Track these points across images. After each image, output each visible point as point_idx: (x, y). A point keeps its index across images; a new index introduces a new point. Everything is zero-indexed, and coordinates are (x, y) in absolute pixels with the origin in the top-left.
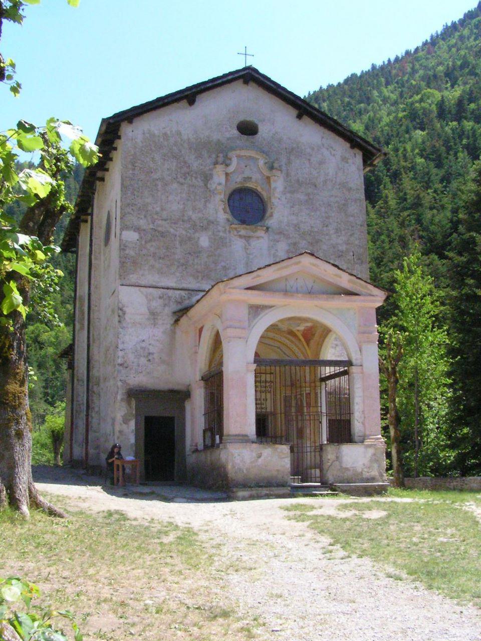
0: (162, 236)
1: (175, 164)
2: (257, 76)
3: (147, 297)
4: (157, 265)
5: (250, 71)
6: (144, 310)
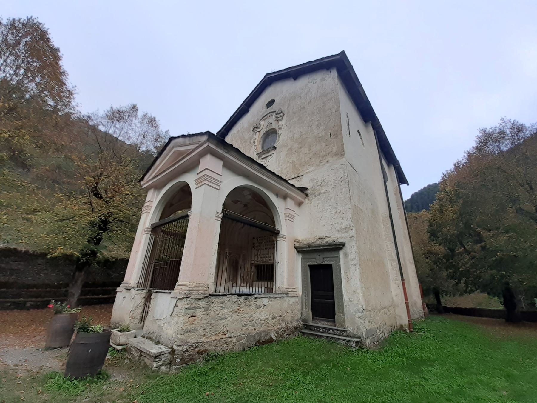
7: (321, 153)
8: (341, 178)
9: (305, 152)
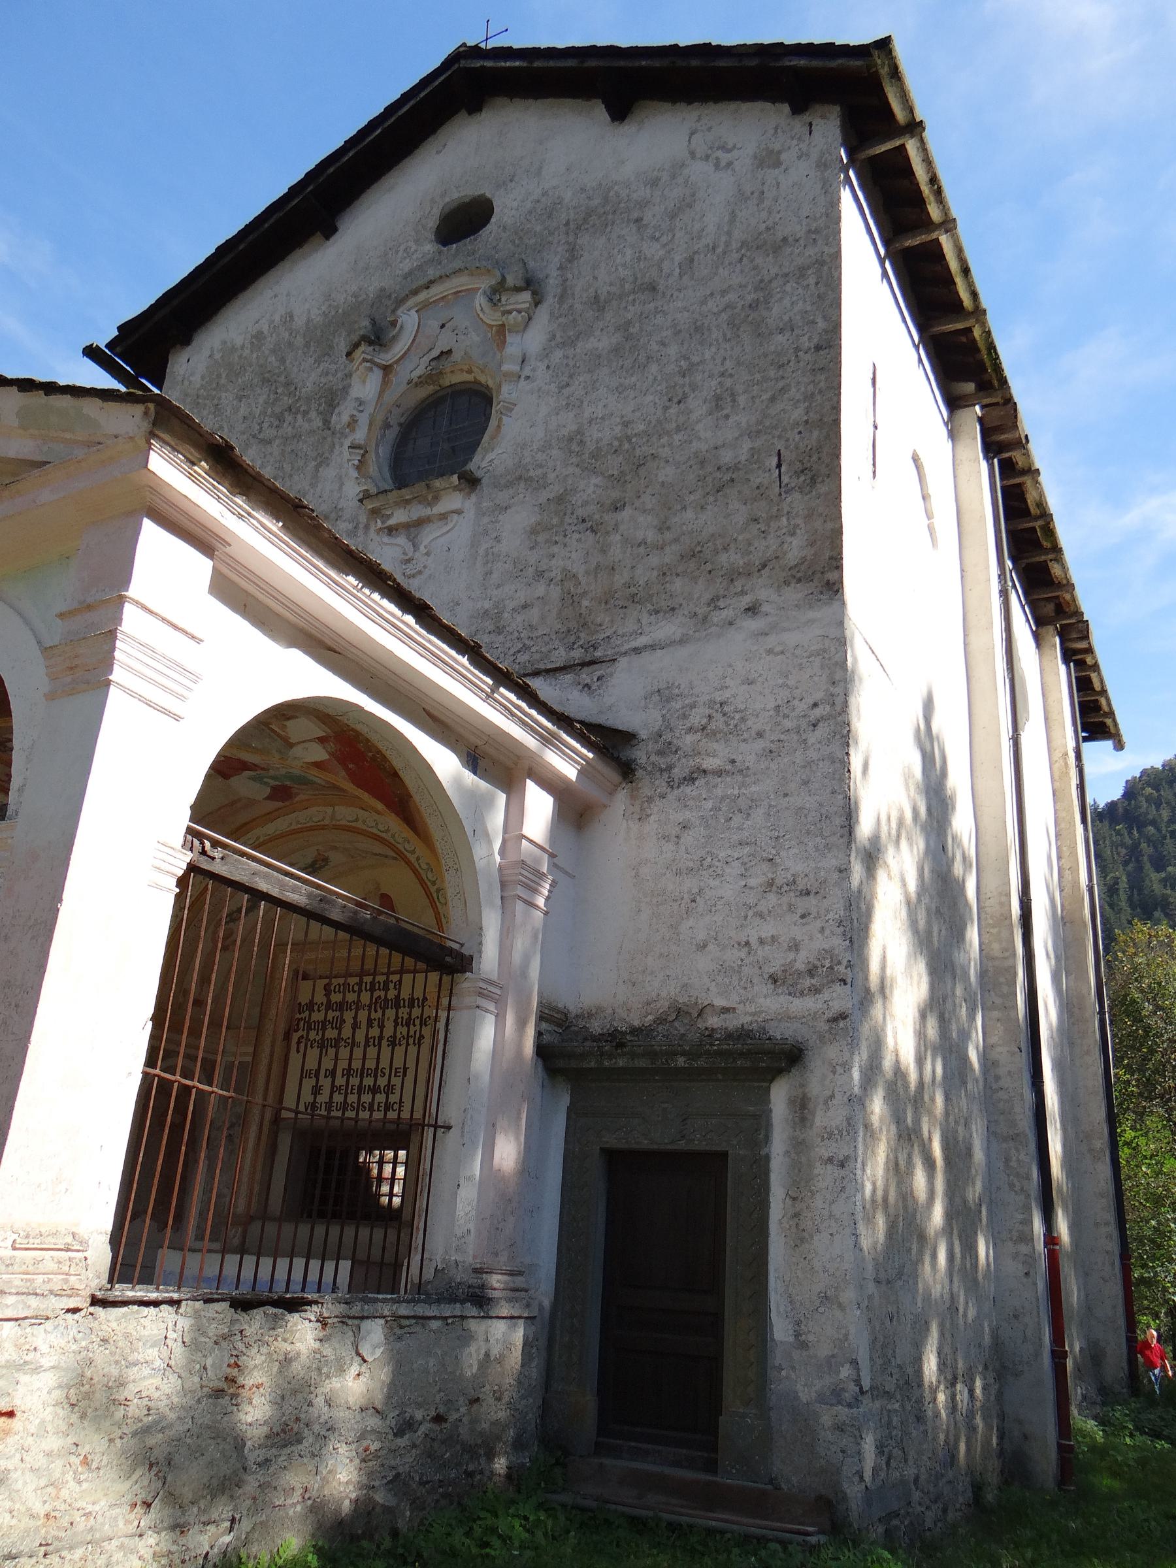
5: (463, 63)
7: (723, 558)
8: (815, 705)
9: (640, 535)
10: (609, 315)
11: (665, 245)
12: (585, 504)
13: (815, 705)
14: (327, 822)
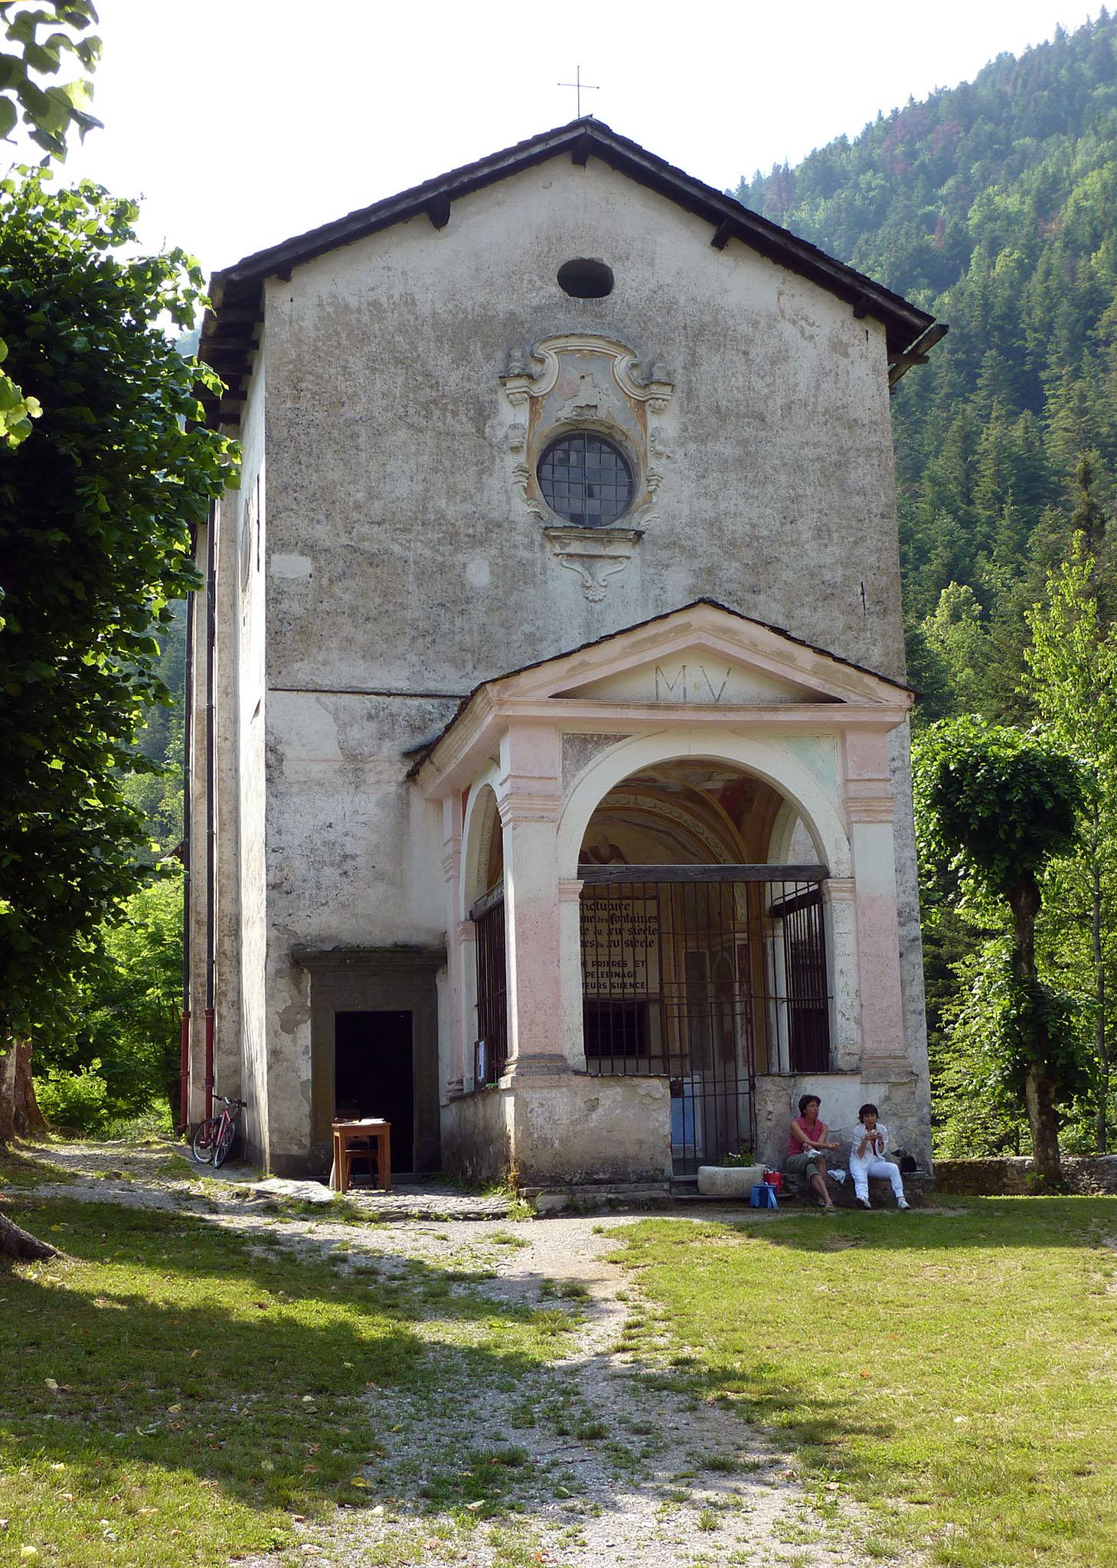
0: (371, 564)
1: (400, 380)
2: (607, 142)
3: (336, 719)
4: (361, 638)
6: (331, 749)
8: (894, 759)
10: (730, 428)
11: (768, 385)
12: (730, 581)
13: (894, 759)
14: (631, 805)
